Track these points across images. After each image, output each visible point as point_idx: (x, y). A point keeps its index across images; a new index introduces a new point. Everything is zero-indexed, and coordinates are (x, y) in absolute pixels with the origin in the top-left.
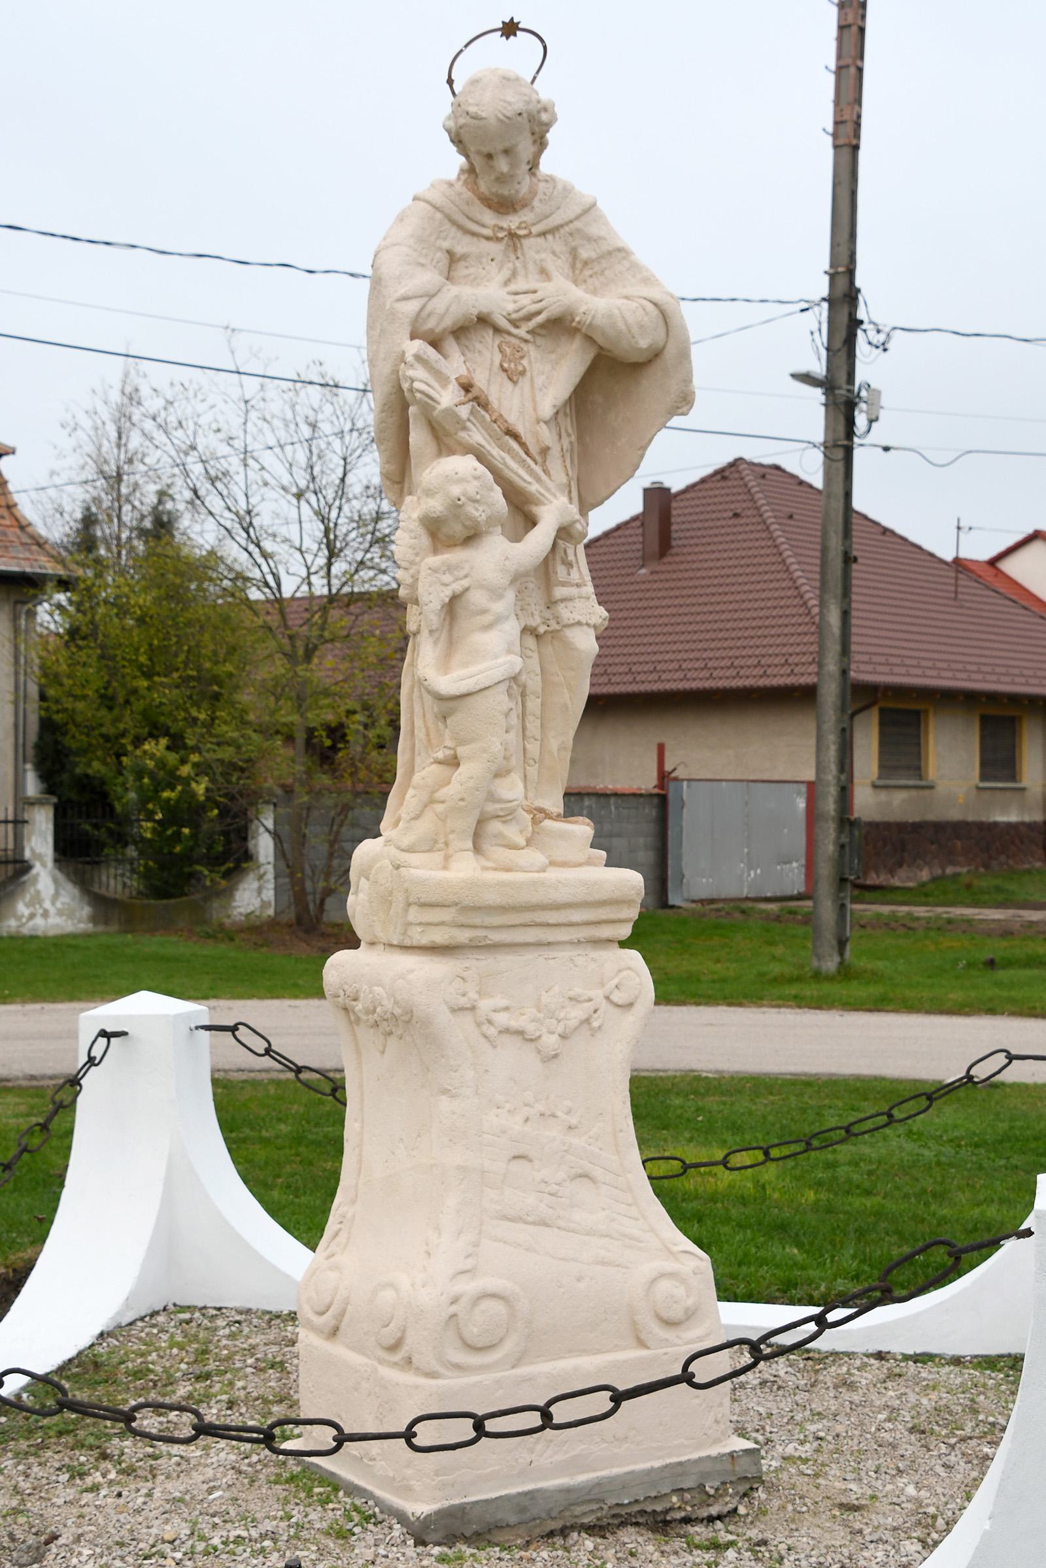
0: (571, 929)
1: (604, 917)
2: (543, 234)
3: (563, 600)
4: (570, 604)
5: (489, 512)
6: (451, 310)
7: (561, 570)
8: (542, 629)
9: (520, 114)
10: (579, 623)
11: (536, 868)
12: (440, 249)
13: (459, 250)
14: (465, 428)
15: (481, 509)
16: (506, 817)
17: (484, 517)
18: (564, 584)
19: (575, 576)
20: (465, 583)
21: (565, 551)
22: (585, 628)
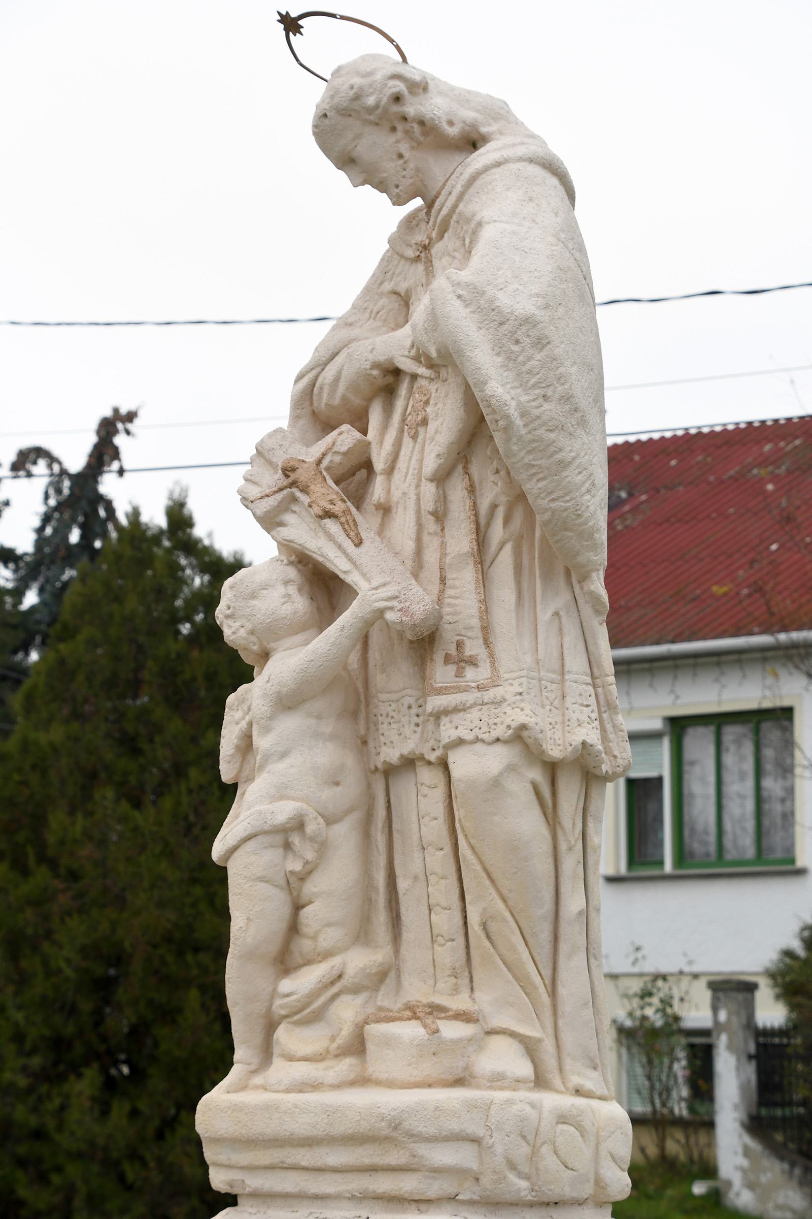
0: (338, 1177)
1: (367, 1161)
2: (441, 236)
3: (446, 712)
4: (457, 718)
5: (249, 626)
6: (344, 372)
7: (442, 674)
8: (432, 757)
9: (325, 115)
10: (460, 742)
11: (282, 1087)
12: (382, 295)
13: (402, 287)
14: (282, 524)
15: (237, 624)
16: (309, 1013)
17: (242, 633)
18: (440, 692)
19: (482, 673)
20: (248, 718)
21: (459, 645)
22: (479, 747)
